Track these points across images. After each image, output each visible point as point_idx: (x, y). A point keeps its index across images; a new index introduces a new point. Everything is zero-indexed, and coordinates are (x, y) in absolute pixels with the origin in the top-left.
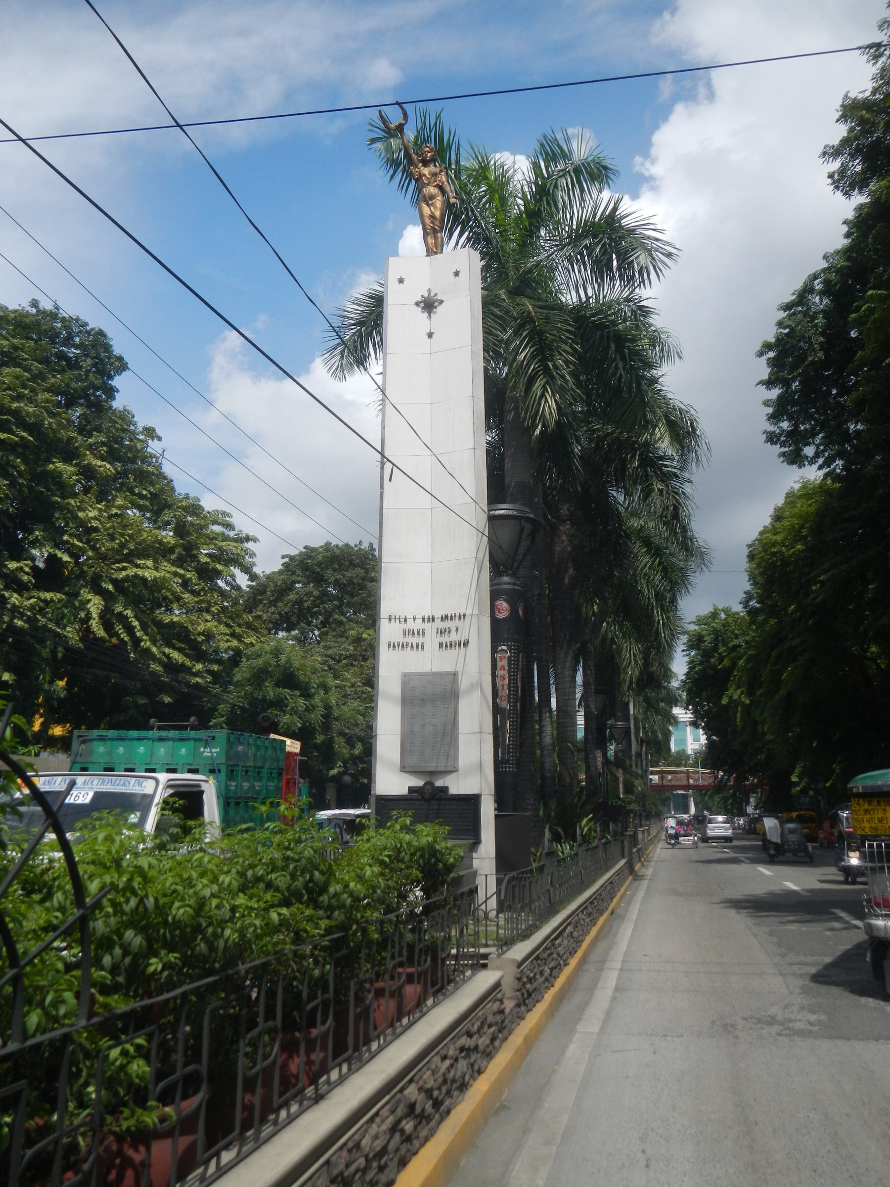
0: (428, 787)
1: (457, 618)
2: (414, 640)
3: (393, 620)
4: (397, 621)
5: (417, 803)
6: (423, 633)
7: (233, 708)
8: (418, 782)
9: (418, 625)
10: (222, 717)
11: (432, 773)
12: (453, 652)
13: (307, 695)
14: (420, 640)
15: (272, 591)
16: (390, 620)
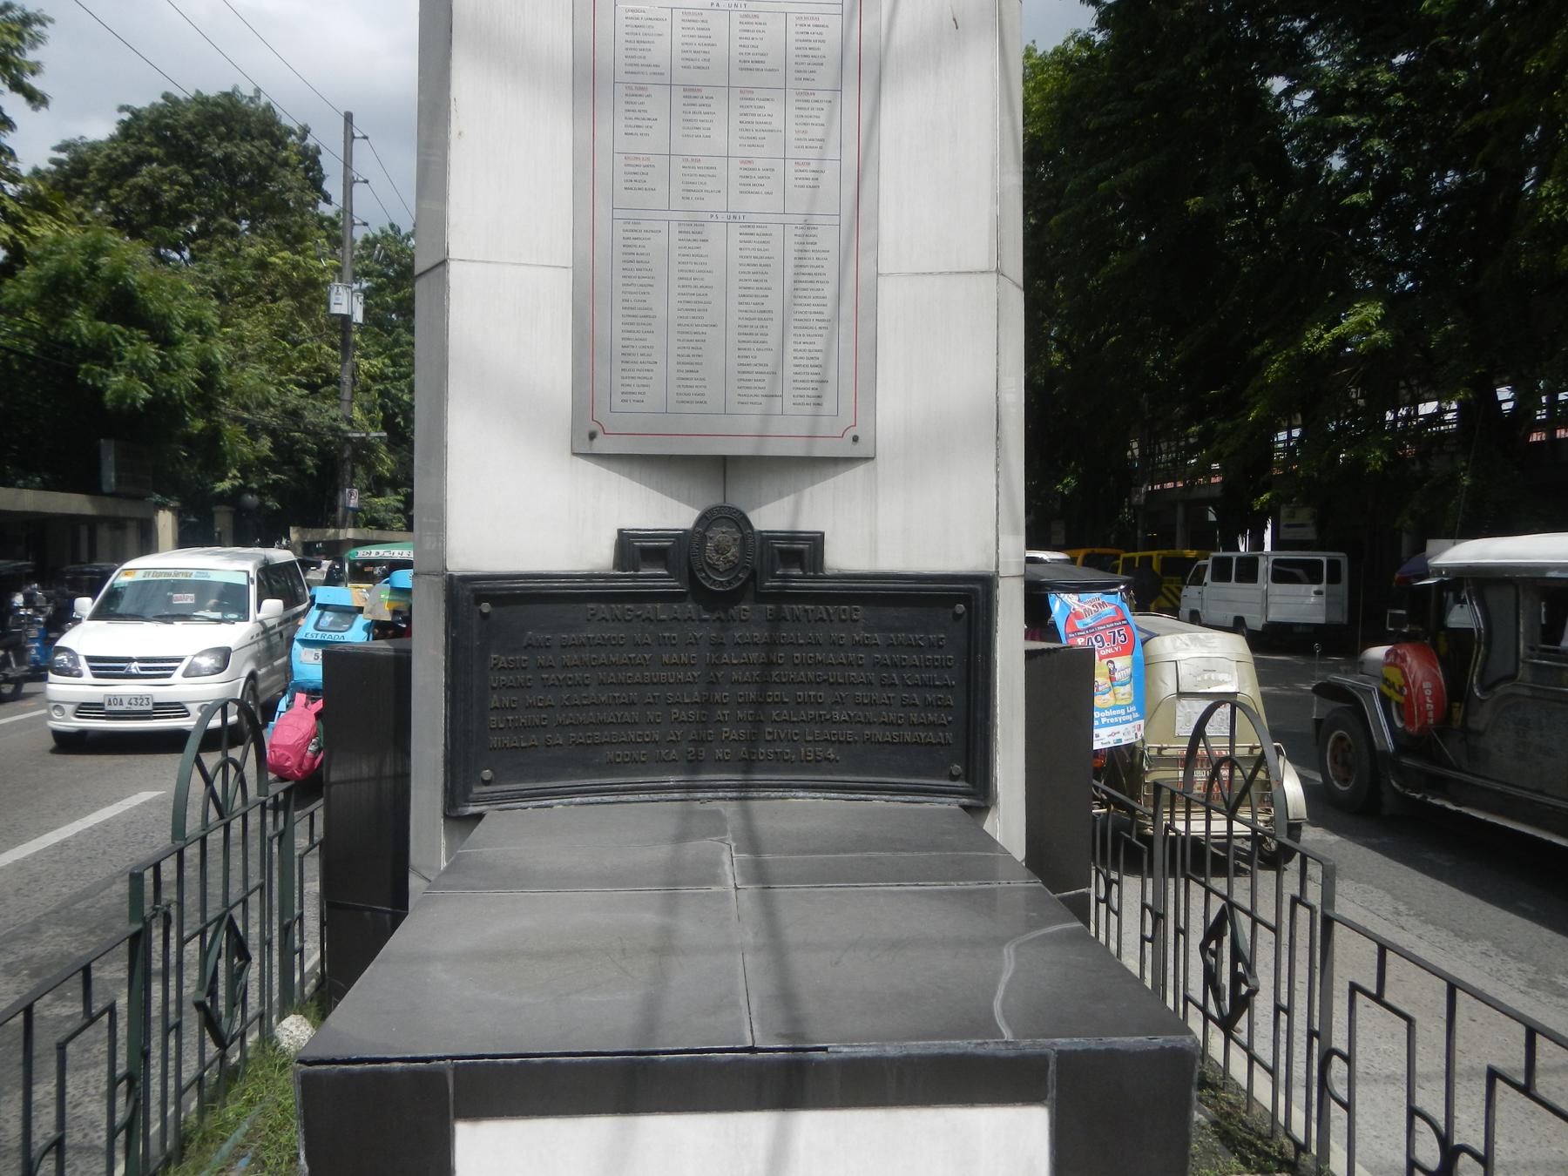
5: (661, 610)
8: (668, 512)
11: (723, 467)
13: (167, 342)
15: (99, 171)
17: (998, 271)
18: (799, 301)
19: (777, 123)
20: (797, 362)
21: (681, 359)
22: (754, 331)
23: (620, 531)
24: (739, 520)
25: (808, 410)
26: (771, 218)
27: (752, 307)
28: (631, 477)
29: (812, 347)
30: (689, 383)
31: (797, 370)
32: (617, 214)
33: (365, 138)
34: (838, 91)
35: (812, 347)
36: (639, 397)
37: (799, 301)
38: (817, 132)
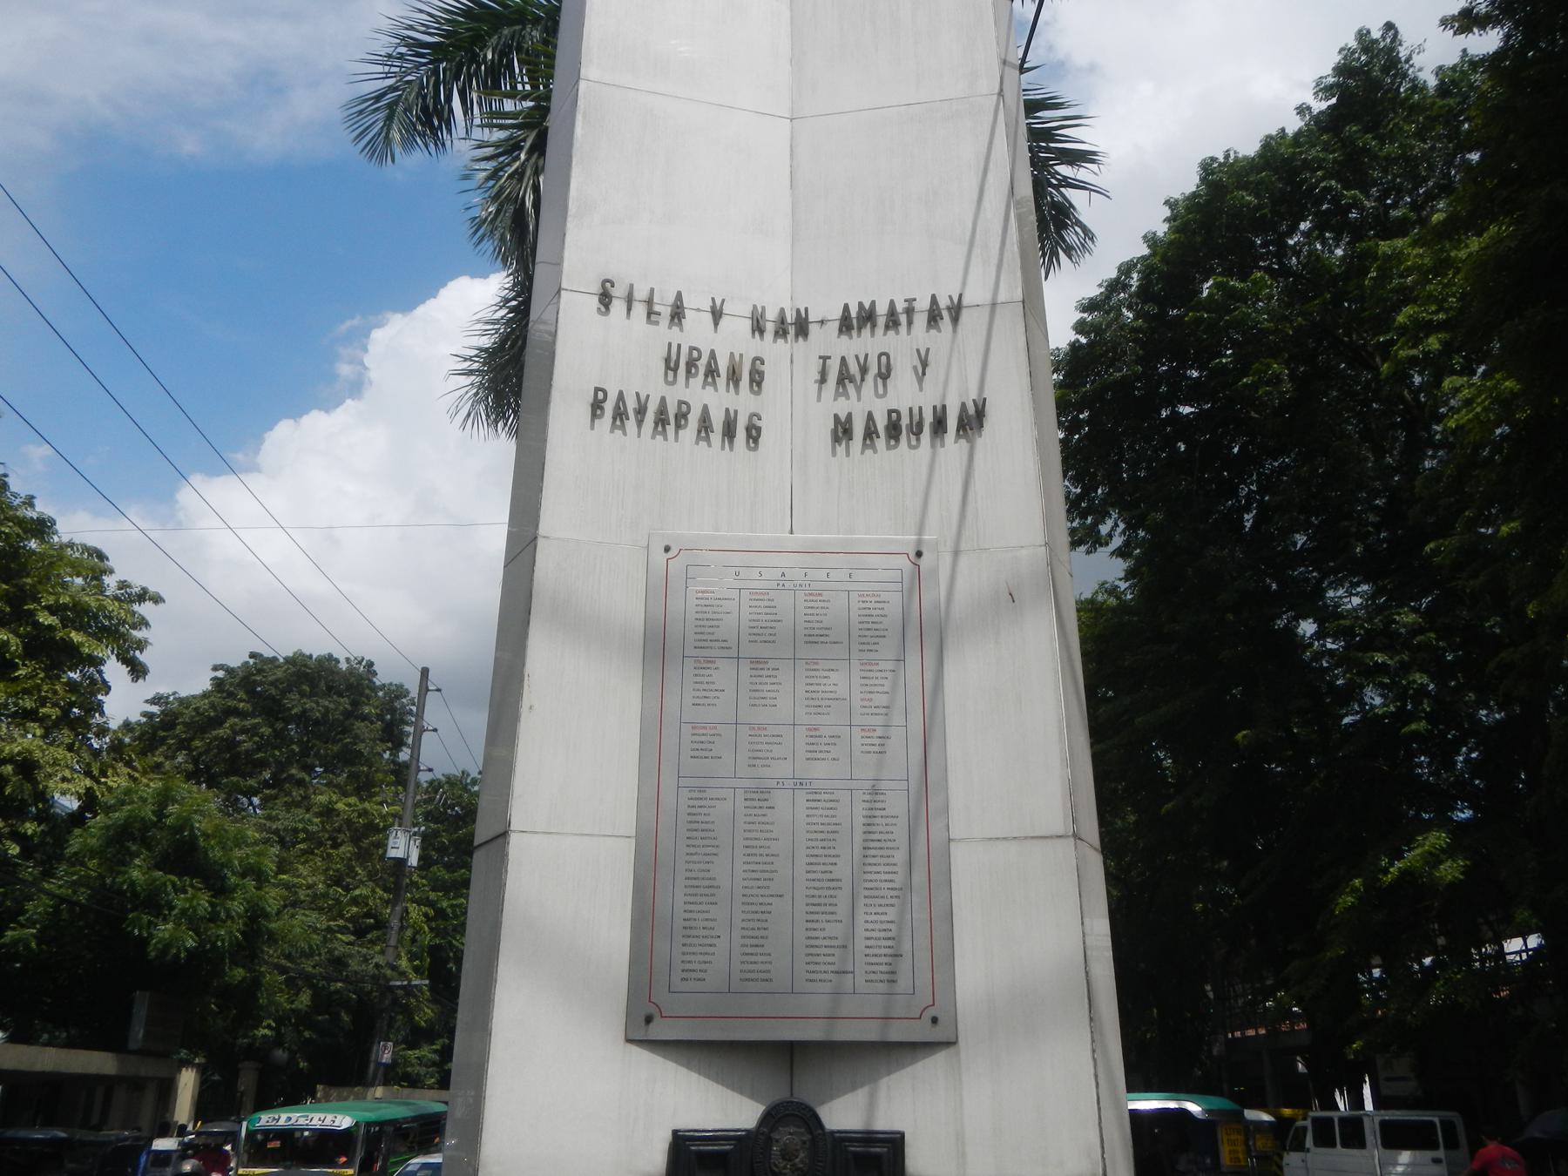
0: (788, 1136)
1: (920, 320)
2: (717, 400)
3: (618, 306)
4: (640, 310)
6: (757, 379)
7: (56, 908)
8: (726, 1109)
9: (733, 340)
10: (32, 924)
11: (790, 1055)
12: (911, 458)
13: (220, 890)
14: (744, 402)
16: (605, 299)
17: (1076, 836)
18: (869, 869)
19: (842, 691)
20: (869, 934)
21: (745, 933)
22: (822, 901)
23: (675, 1132)
24: (809, 1119)
25: (882, 987)
26: (838, 784)
27: (820, 876)
28: (688, 1066)
29: (884, 918)
30: (753, 959)
31: (869, 943)
32: (683, 782)
33: (435, 730)
34: (901, 660)
35: (884, 918)
36: (701, 975)
37: (869, 869)
38: (882, 700)
